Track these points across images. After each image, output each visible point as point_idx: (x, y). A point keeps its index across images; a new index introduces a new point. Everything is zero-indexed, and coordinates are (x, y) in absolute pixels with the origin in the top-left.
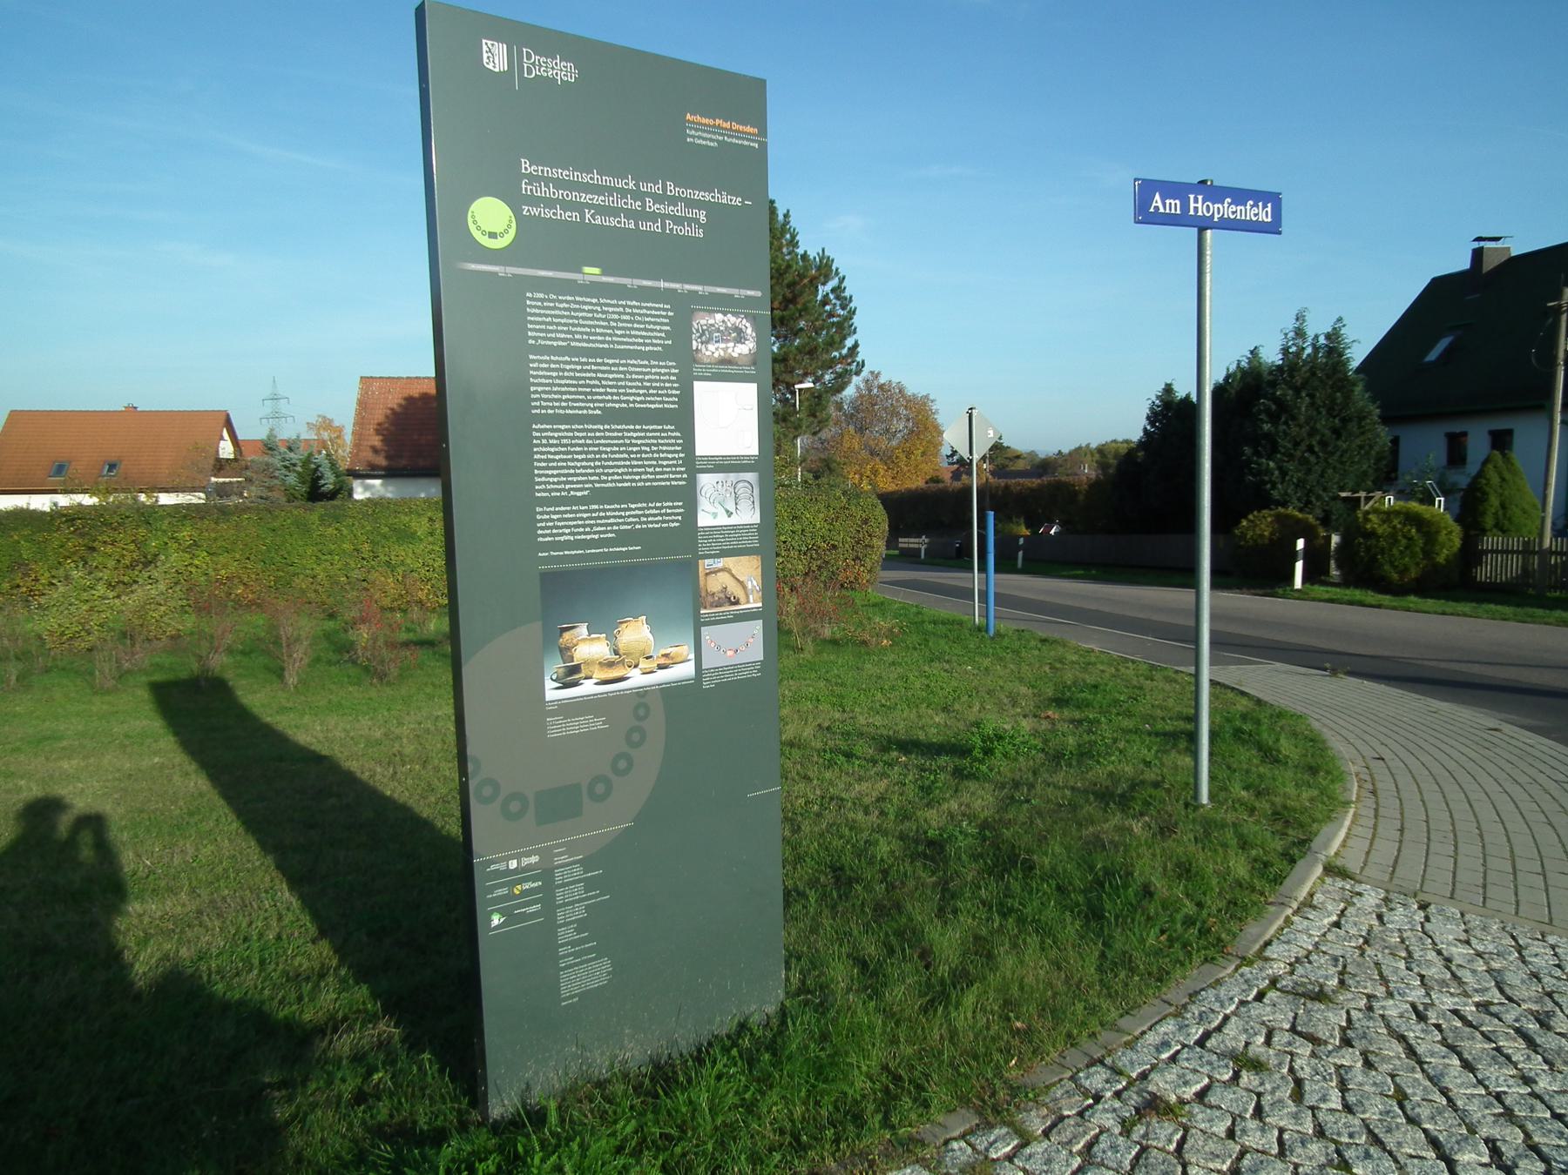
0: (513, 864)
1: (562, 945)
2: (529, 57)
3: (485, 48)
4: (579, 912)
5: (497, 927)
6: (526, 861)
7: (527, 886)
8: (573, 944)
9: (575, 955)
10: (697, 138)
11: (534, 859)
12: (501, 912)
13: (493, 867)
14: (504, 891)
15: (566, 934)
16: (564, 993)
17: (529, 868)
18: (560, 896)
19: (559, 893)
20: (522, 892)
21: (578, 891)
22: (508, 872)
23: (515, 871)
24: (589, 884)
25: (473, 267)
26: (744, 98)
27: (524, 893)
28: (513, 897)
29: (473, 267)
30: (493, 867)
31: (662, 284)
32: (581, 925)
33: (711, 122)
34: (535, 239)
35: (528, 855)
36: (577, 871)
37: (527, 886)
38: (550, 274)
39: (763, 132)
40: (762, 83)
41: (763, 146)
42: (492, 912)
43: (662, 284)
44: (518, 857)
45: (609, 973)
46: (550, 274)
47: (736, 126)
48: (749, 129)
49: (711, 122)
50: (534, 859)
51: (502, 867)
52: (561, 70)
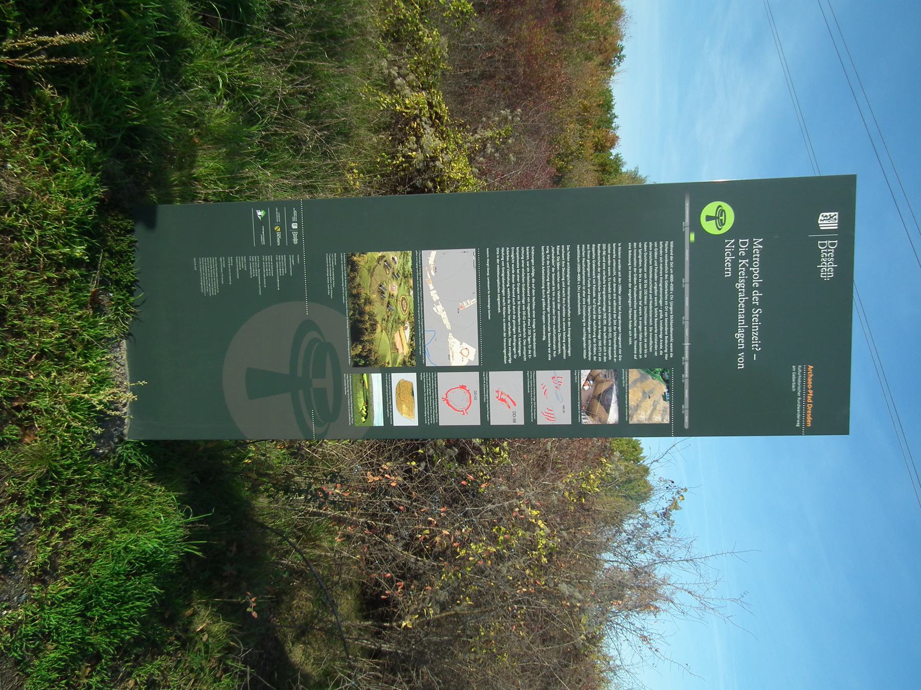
0: (295, 226)
1: (234, 259)
2: (833, 245)
3: (833, 214)
4: (254, 272)
6: (295, 235)
7: (279, 235)
8: (234, 268)
9: (226, 270)
10: (796, 372)
11: (295, 241)
12: (266, 216)
13: (295, 212)
15: (241, 262)
16: (202, 260)
17: (291, 237)
19: (269, 258)
20: (276, 231)
21: (268, 272)
22: (290, 222)
24: (271, 280)
25: (687, 205)
26: (832, 418)
27: (274, 232)
29: (687, 205)
30: (295, 212)
31: (687, 344)
32: (245, 273)
33: (810, 386)
34: (710, 246)
35: (299, 237)
36: (282, 271)
37: (279, 235)
38: (687, 258)
39: (810, 431)
40: (846, 432)
41: (798, 432)
42: (266, 211)
43: (687, 344)
44: (299, 230)
45: (208, 293)
46: (687, 258)
47: (810, 407)
48: (809, 419)
49: (810, 386)
50: (295, 241)
51: (294, 219)
52: (827, 268)
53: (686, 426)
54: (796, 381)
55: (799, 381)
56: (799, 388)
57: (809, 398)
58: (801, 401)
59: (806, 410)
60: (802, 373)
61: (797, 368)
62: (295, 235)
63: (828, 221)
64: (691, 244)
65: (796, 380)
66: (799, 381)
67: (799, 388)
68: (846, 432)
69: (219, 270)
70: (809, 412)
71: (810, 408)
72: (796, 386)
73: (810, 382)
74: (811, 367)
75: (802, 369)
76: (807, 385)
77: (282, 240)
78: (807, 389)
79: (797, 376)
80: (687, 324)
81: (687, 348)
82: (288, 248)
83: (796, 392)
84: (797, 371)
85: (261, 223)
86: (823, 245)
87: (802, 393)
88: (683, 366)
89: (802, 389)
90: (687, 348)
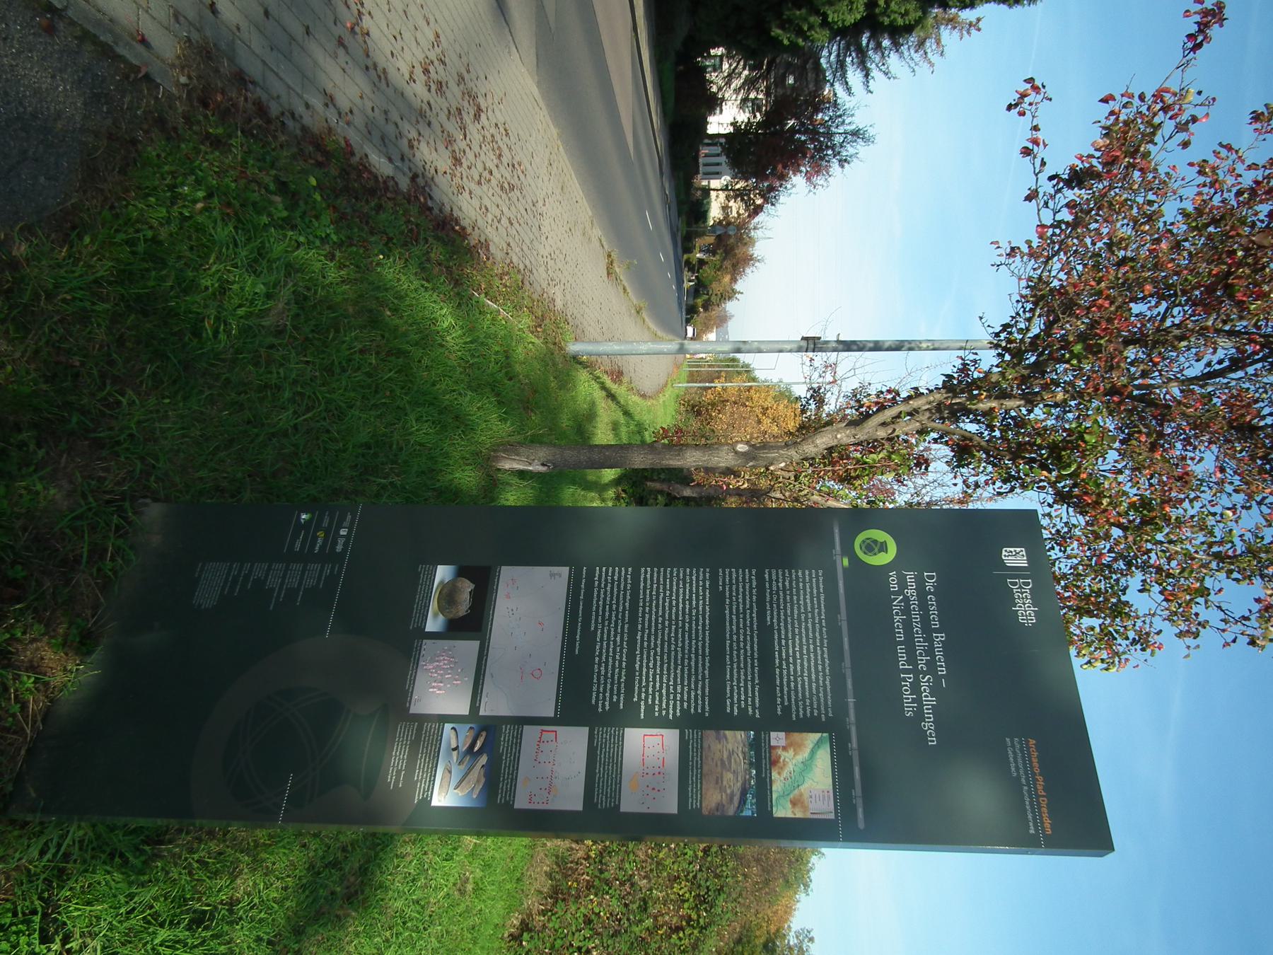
1: (252, 566)
5: (299, 516)
6: (341, 542)
8: (247, 577)
11: (339, 548)
12: (308, 522)
13: (349, 517)
14: (325, 523)
17: (335, 543)
18: (297, 567)
19: (299, 567)
22: (340, 527)
23: (337, 532)
25: (836, 531)
27: (315, 538)
28: (315, 532)
29: (836, 531)
30: (349, 517)
35: (346, 545)
38: (841, 590)
42: (313, 514)
44: (348, 537)
45: (200, 605)
46: (841, 590)
50: (339, 548)
51: (346, 524)
53: (861, 825)
54: (1016, 762)
55: (1020, 761)
56: (1021, 772)
57: (1040, 788)
58: (1029, 792)
59: (1040, 808)
60: (1022, 750)
61: (1012, 742)
62: (341, 542)
63: (1015, 557)
64: (845, 569)
65: (1016, 762)
66: (1020, 761)
67: (1021, 772)
68: (1110, 848)
69: (227, 579)
70: (1045, 810)
71: (1044, 804)
72: (1017, 768)
73: (1036, 764)
74: (1032, 742)
75: (1020, 743)
76: (1032, 767)
77: (323, 547)
78: (1034, 774)
79: (1014, 753)
80: (849, 673)
81: (851, 706)
82: (328, 556)
83: (1019, 777)
84: (1013, 746)
85: (300, 526)
86: (1015, 584)
87: (1027, 779)
88: (849, 732)
89: (1026, 774)
90: (851, 706)
